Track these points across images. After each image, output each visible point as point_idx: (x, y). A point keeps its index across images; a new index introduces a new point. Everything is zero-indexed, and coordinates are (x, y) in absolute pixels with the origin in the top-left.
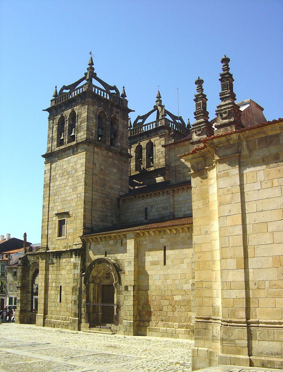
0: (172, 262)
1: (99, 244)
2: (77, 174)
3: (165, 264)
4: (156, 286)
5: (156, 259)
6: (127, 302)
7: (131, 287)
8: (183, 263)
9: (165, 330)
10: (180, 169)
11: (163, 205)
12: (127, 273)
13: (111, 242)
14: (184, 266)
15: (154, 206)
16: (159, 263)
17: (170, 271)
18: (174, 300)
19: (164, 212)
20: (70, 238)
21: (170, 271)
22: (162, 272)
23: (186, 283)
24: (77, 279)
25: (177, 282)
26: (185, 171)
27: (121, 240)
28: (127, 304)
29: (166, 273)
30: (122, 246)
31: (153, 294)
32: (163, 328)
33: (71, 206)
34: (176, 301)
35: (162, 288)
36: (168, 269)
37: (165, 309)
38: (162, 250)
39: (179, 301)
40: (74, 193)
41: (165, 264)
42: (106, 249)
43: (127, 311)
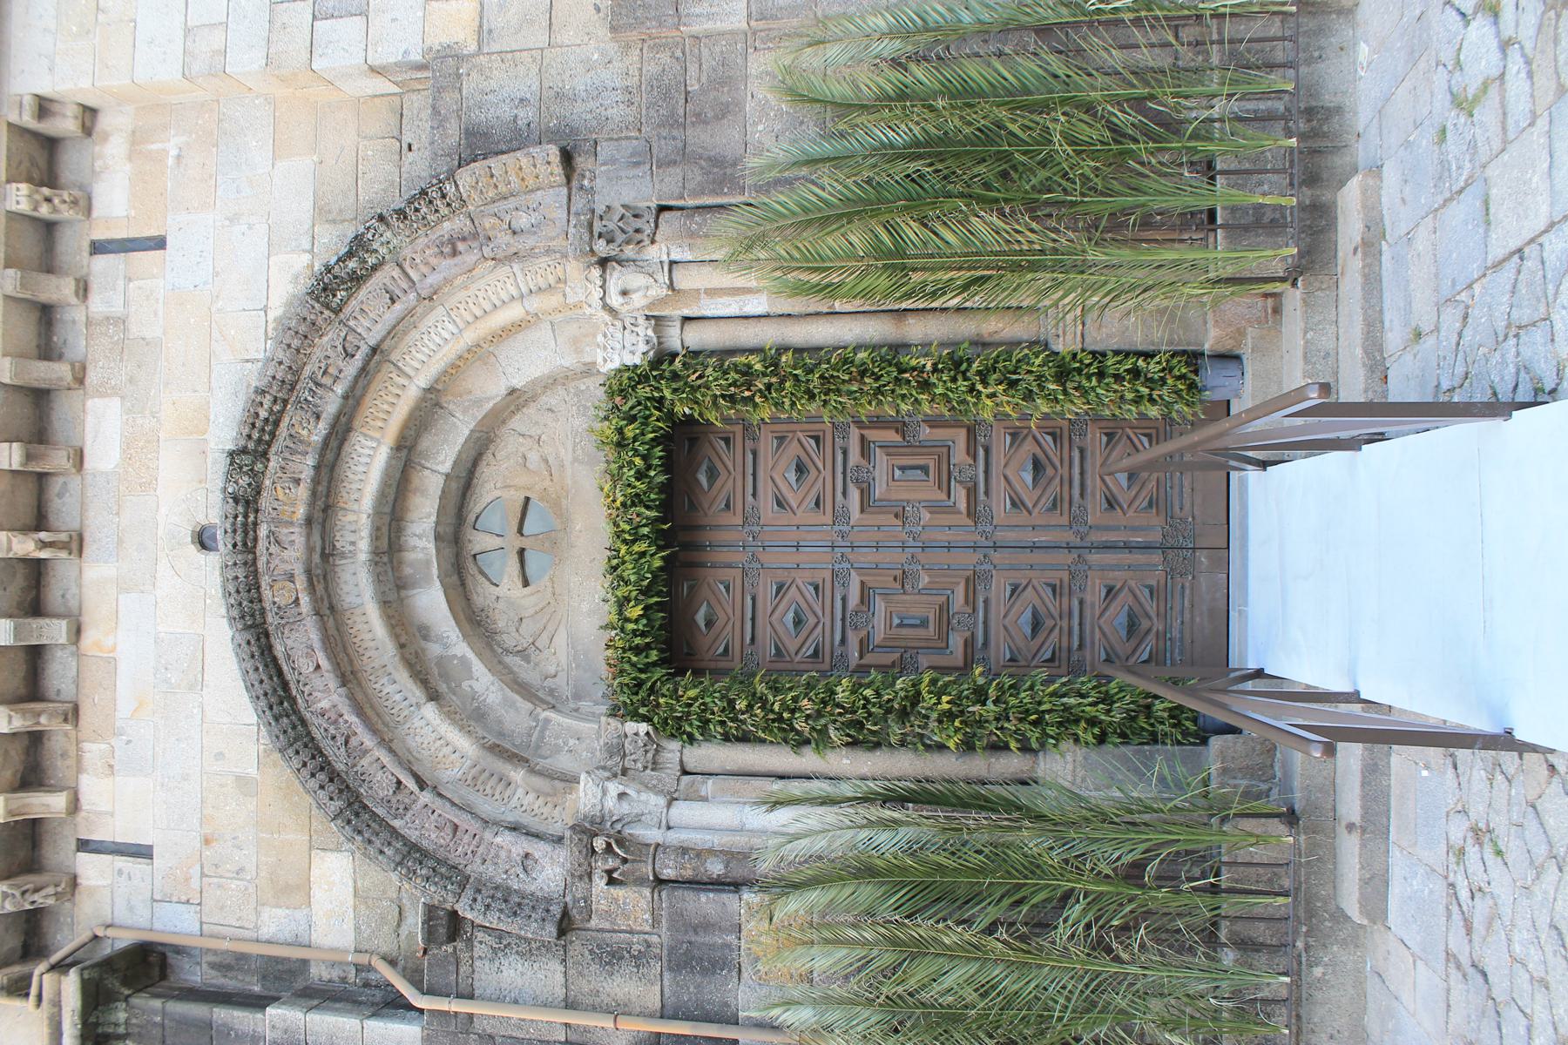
27: (101, 262)
30: (159, 243)
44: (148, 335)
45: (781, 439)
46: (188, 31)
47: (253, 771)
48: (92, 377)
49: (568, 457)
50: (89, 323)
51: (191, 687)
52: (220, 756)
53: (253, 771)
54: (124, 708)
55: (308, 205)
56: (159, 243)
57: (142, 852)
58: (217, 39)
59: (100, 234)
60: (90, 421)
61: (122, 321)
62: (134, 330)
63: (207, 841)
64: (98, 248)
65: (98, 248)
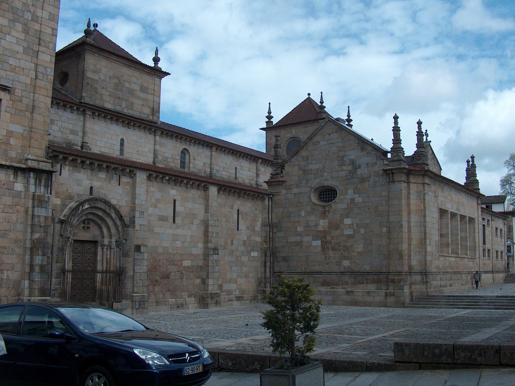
0: (182, 220)
1: (80, 173)
2: (37, 27)
3: (174, 221)
4: (163, 247)
5: (164, 214)
6: (139, 267)
7: (145, 247)
8: (193, 224)
9: (175, 302)
10: (98, 86)
11: (71, 126)
12: (137, 227)
13: (103, 175)
14: (194, 227)
15: (56, 121)
16: (168, 219)
17: (179, 231)
18: (183, 265)
19: (71, 137)
20: (12, 141)
21: (179, 231)
22: (170, 231)
23: (194, 247)
24: (44, 226)
25: (186, 245)
26: (103, 93)
27: (118, 176)
28: (139, 271)
29: (175, 233)
30: (119, 185)
31: (161, 258)
32: (172, 300)
33: (17, 79)
34: (185, 267)
35: (170, 250)
36: (177, 227)
37: (172, 276)
38: (172, 204)
39: (188, 267)
40: (25, 57)
41: (174, 221)
42: (91, 184)
43: (138, 281)
44: (111, 182)
45: (92, 257)
46: (140, 194)
47: (69, 192)
48: (108, 174)
49: (94, 233)
50: (113, 174)
51: (77, 184)
52: (70, 187)
53: (69, 192)
54: (76, 174)
55: (121, 205)
56: (119, 185)
57: (60, 175)
58: (139, 198)
59: (121, 176)
60: (103, 173)
61: (113, 179)
62: (112, 180)
63: (62, 184)
64: (120, 176)
65: (120, 176)
